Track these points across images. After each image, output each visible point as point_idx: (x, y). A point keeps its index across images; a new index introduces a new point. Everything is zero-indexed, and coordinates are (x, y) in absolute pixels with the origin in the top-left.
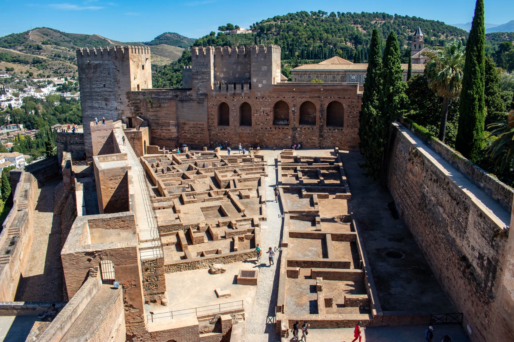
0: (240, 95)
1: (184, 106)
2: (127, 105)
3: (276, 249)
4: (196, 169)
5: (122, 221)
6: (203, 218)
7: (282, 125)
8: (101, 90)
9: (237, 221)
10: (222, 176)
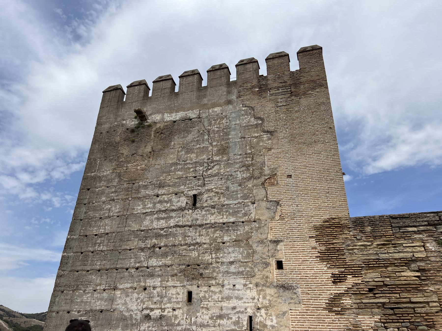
2: (323, 302)
8: (172, 223)
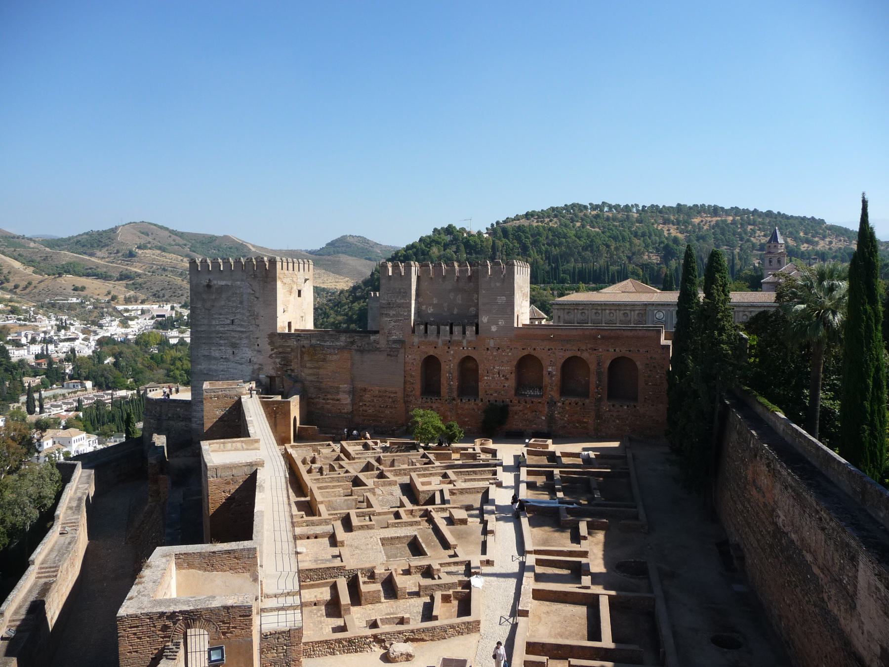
0: (459, 343)
3: (503, 620)
4: (378, 469)
5: (235, 558)
6: (382, 557)
7: (530, 395)
8: (226, 329)
9: (441, 565)
10: (423, 484)
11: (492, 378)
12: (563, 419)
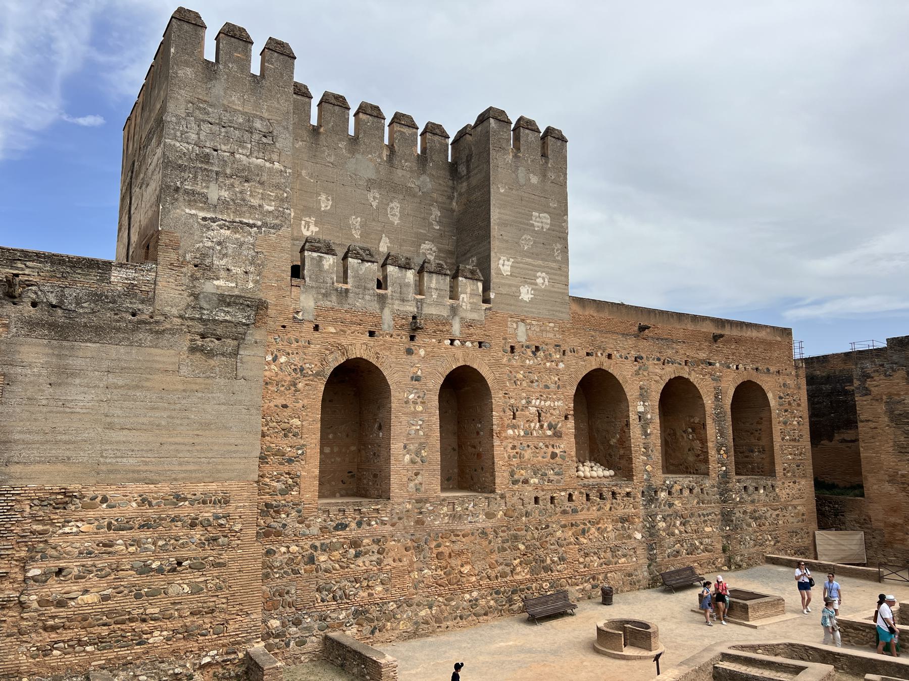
1: (76, 362)
11: (526, 434)
12: (673, 534)
